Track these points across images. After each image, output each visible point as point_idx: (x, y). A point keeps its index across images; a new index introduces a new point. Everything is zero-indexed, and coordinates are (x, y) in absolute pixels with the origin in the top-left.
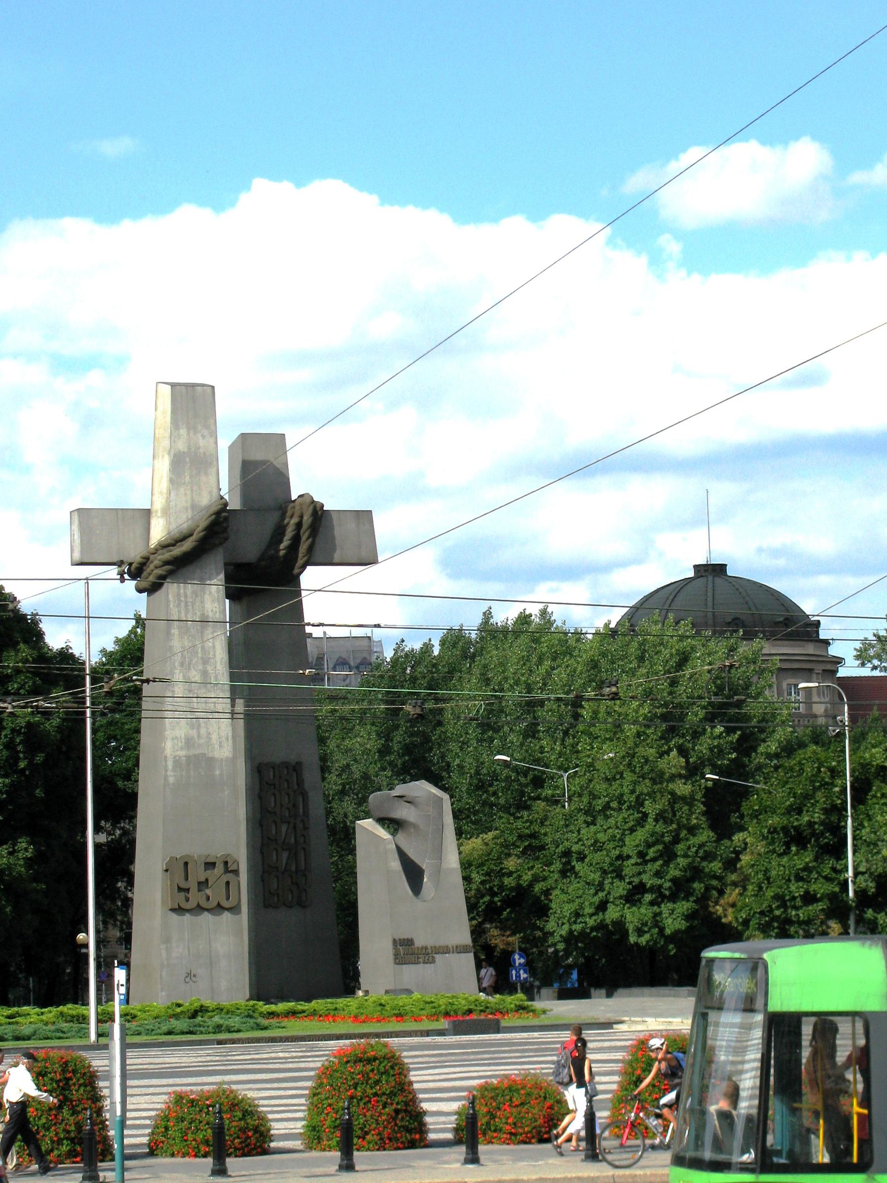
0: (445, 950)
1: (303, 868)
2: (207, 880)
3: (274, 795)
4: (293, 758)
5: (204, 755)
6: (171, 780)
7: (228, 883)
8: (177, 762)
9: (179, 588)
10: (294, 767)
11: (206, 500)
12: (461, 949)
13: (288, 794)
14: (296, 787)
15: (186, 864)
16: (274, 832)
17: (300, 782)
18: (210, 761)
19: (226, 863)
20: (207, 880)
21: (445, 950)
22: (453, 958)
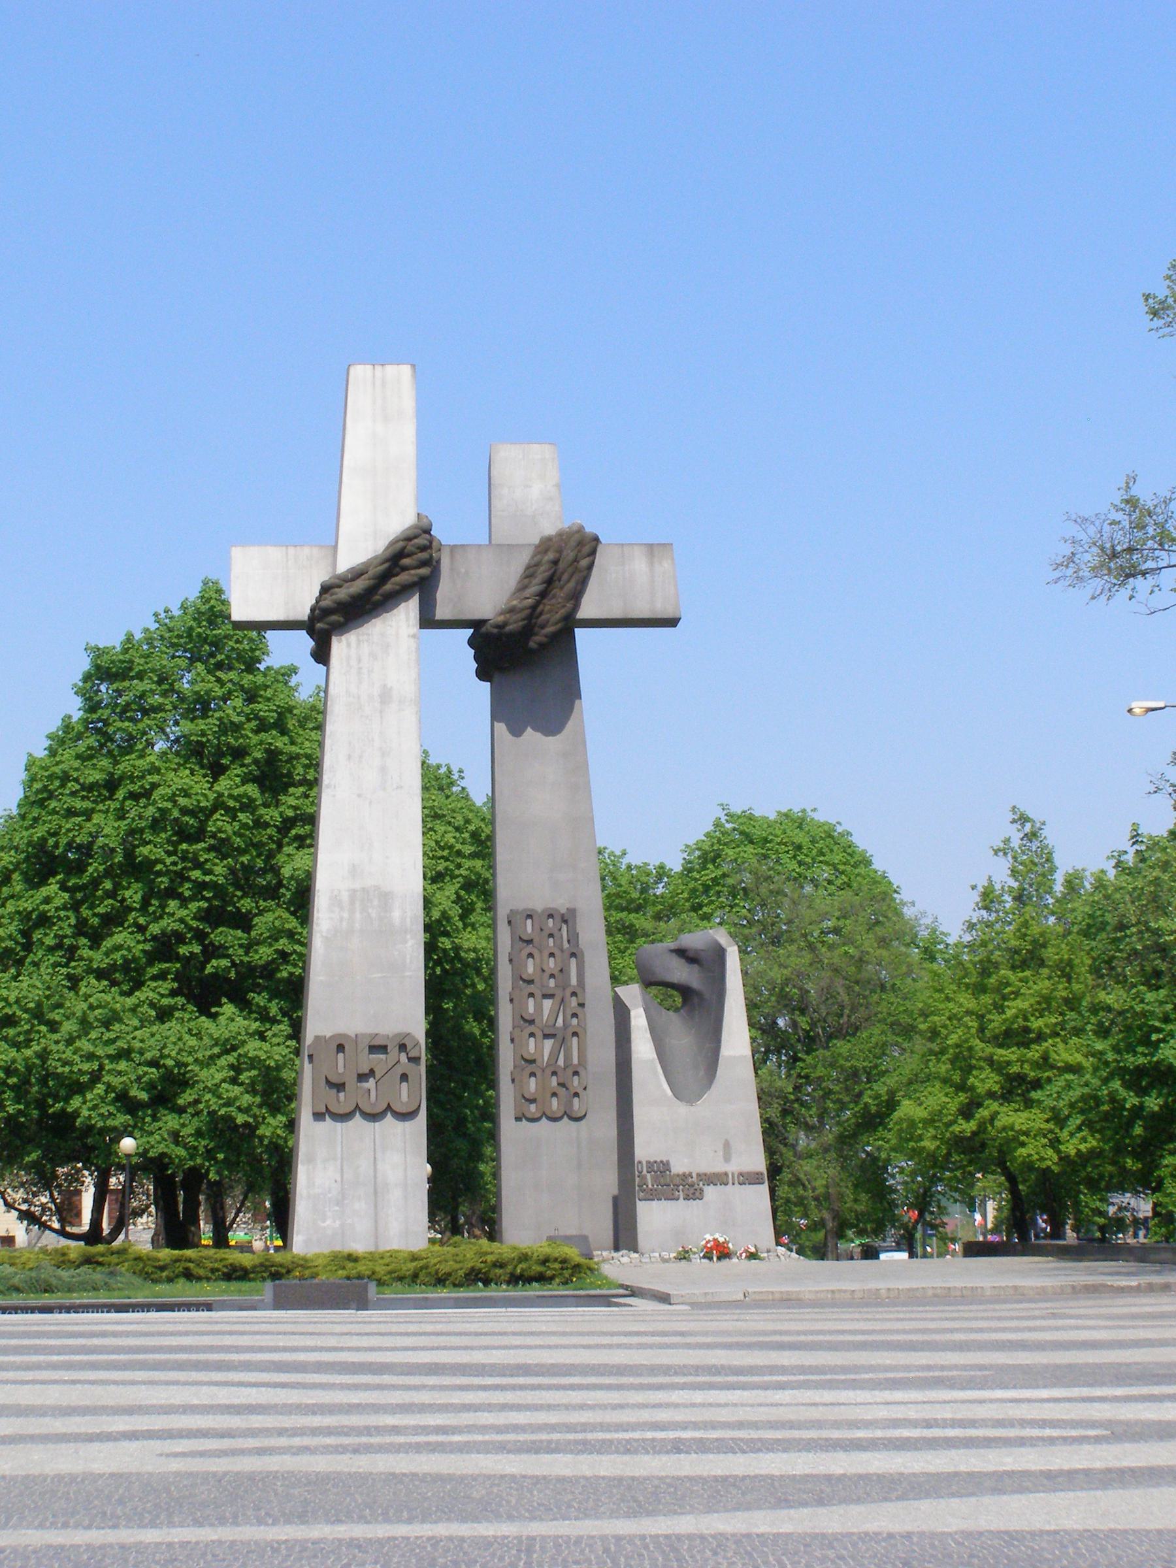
0: (718, 1179)
1: (575, 1061)
4: (561, 904)
5: (377, 888)
10: (563, 915)
12: (748, 1179)
14: (566, 945)
15: (341, 1048)
17: (573, 938)
18: (386, 898)
19: (403, 1047)
20: (372, 1072)
21: (718, 1179)
22: (735, 1192)
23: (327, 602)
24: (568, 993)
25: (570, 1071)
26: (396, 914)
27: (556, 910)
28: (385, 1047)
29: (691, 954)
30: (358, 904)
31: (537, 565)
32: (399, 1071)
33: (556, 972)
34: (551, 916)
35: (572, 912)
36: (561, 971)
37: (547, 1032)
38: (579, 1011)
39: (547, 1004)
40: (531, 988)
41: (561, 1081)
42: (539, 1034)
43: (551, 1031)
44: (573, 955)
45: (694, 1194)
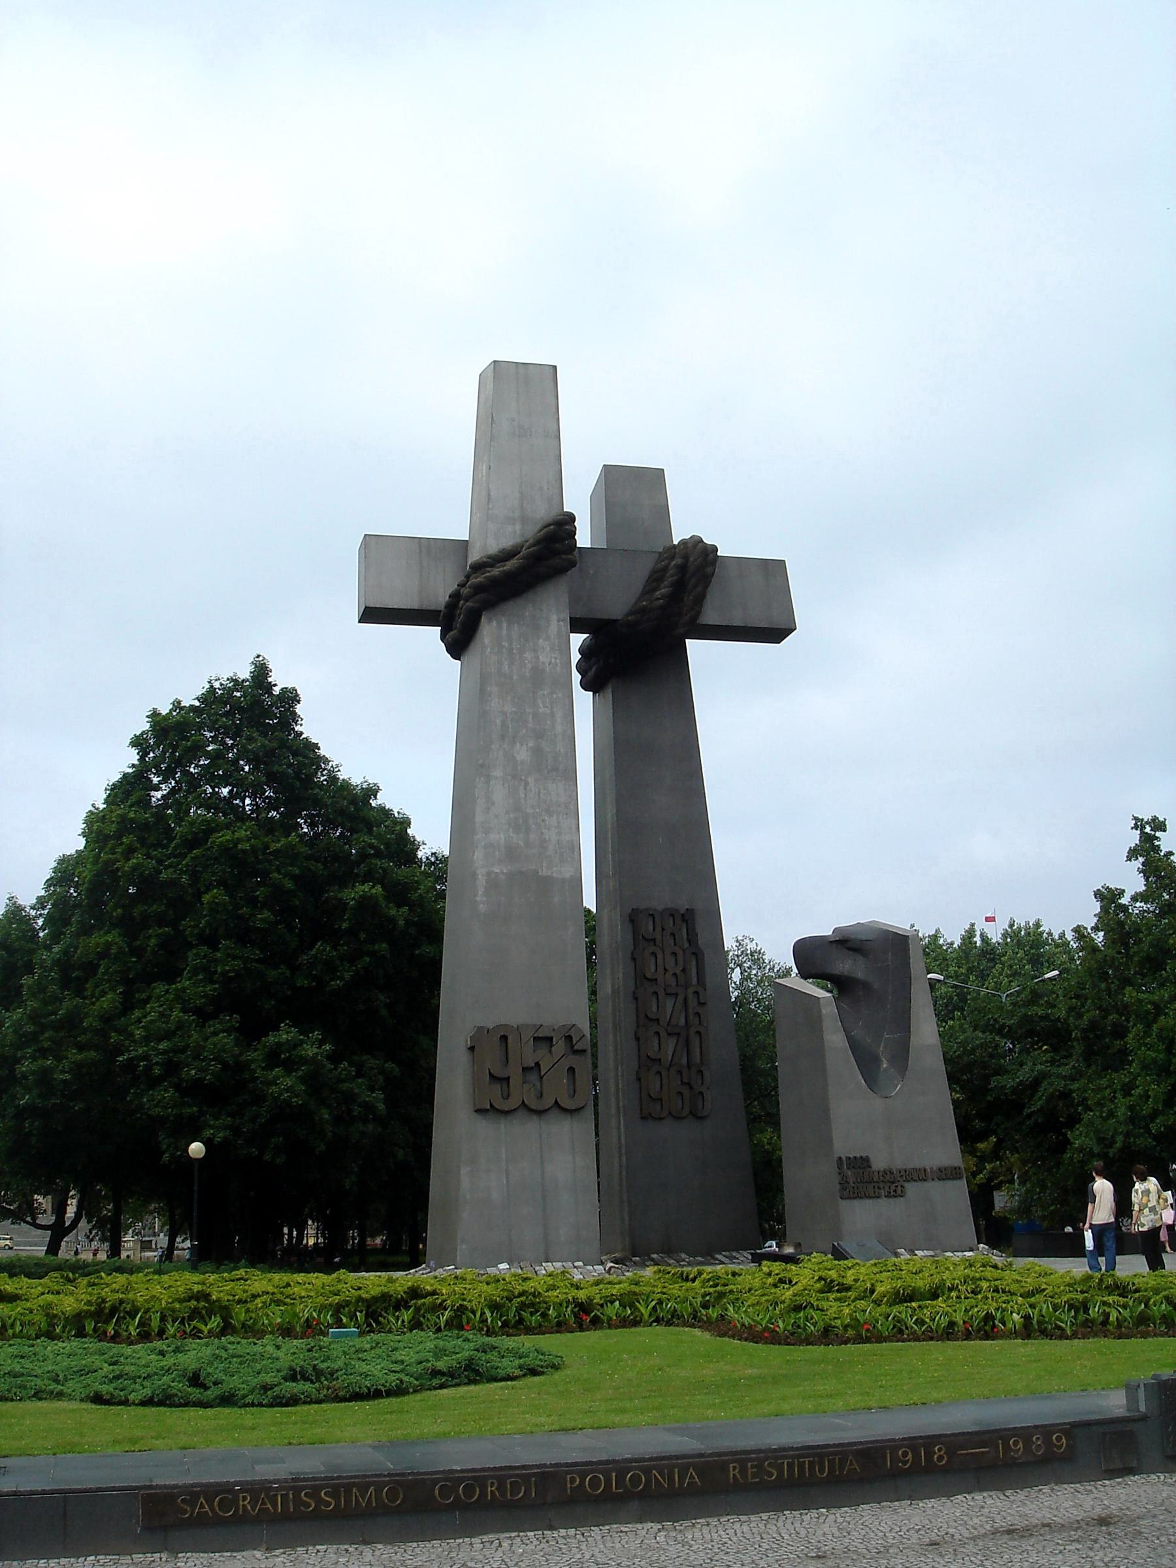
0: (920, 1175)
1: (698, 1061)
2: (537, 1064)
3: (653, 953)
4: (682, 904)
6: (482, 908)
7: (571, 1070)
8: (492, 883)
9: (500, 627)
11: (542, 513)
12: (947, 1174)
13: (674, 954)
14: (686, 945)
15: (504, 1038)
16: (654, 1009)
17: (692, 939)
19: (569, 1038)
22: (934, 1189)
23: (478, 579)
27: (677, 910)
28: (551, 1039)
31: (665, 569)
32: (566, 1063)
33: (678, 972)
35: (691, 911)
36: (683, 970)
41: (685, 1080)
42: (663, 1034)
45: (896, 1192)
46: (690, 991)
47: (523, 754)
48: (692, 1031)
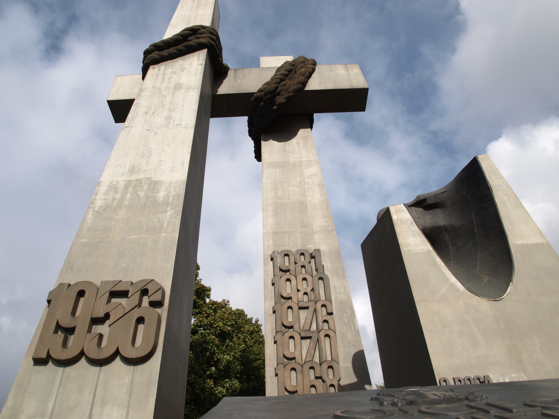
1: (329, 358)
4: (311, 248)
5: (150, 179)
14: (315, 273)
17: (319, 268)
18: (154, 185)
19: (145, 292)
20: (107, 316)
24: (319, 305)
25: (325, 366)
26: (161, 194)
29: (429, 202)
30: (130, 189)
33: (308, 291)
34: (302, 254)
36: (312, 290)
37: (303, 335)
38: (328, 318)
39: (303, 314)
40: (289, 303)
41: (318, 375)
42: (297, 337)
43: (308, 335)
44: (321, 278)
46: (319, 305)
47: (159, 120)
48: (322, 334)
